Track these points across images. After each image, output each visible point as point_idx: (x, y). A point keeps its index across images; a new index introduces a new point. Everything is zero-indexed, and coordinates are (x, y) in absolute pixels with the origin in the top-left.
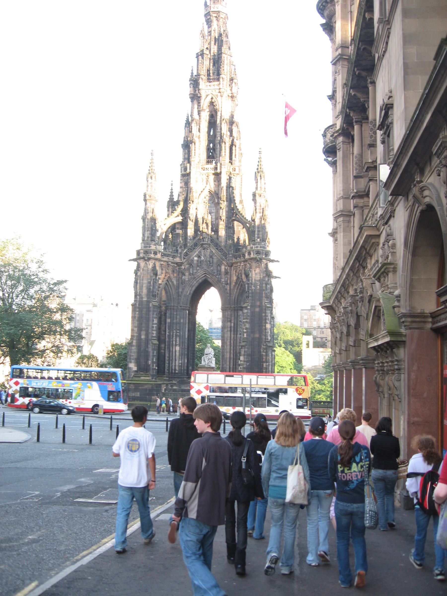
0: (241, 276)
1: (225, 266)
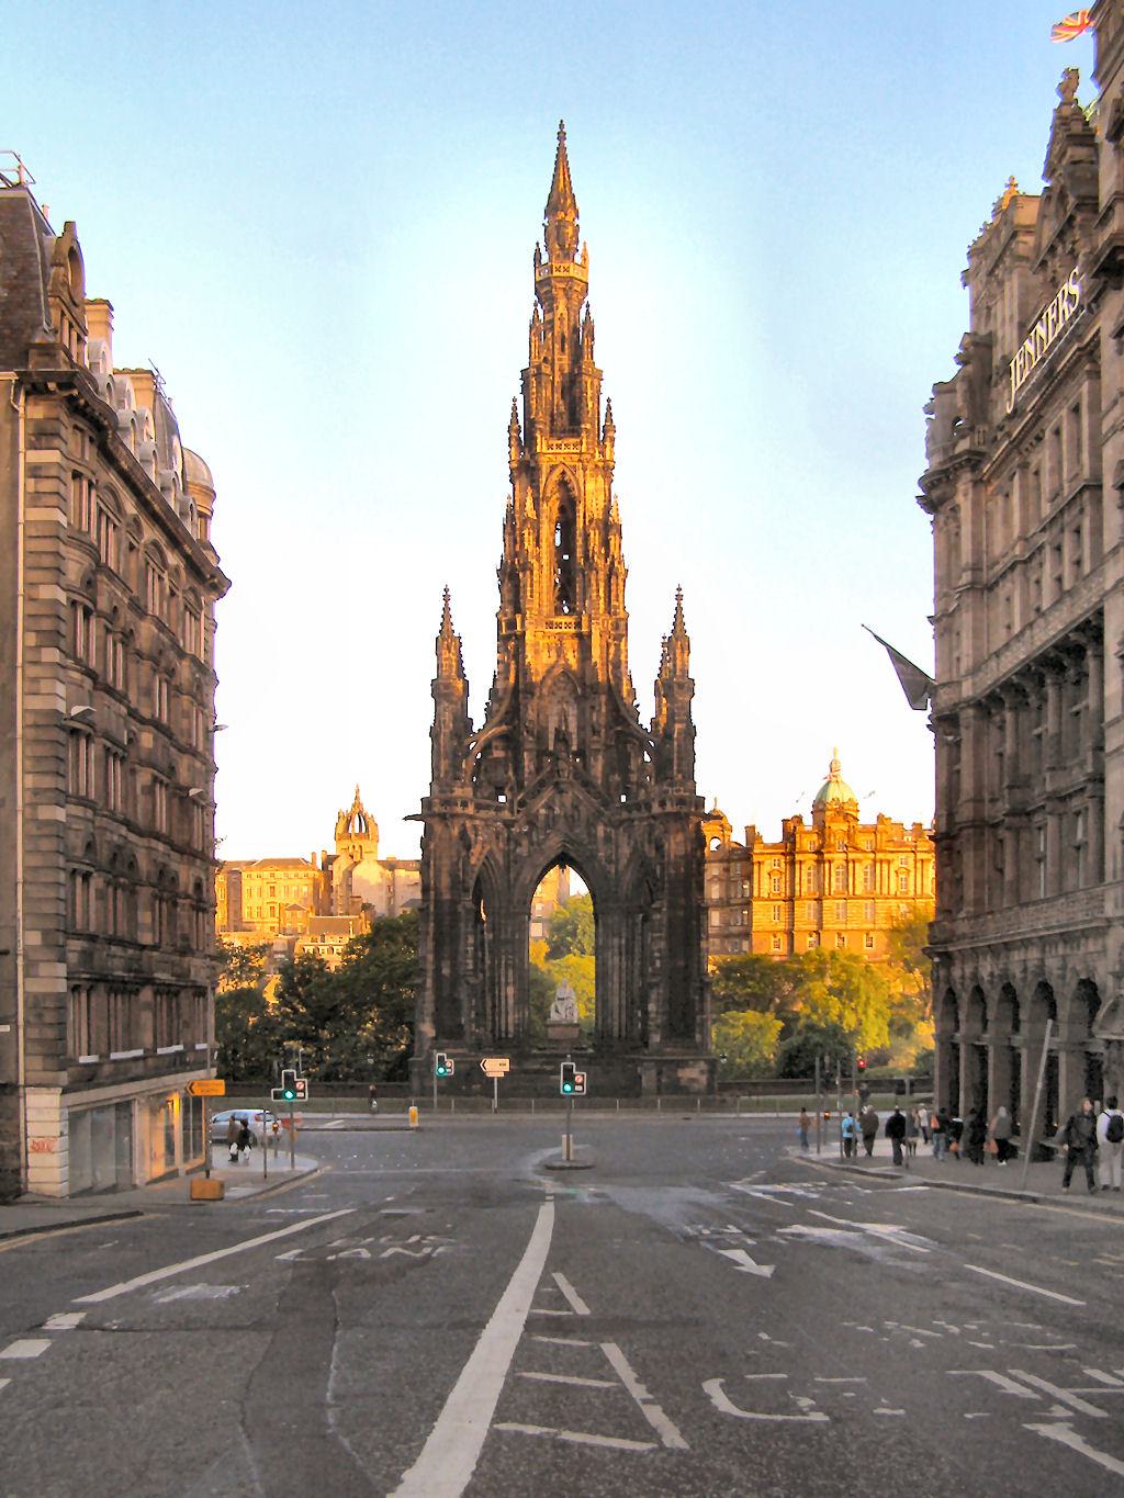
0: (643, 846)
1: (605, 825)
